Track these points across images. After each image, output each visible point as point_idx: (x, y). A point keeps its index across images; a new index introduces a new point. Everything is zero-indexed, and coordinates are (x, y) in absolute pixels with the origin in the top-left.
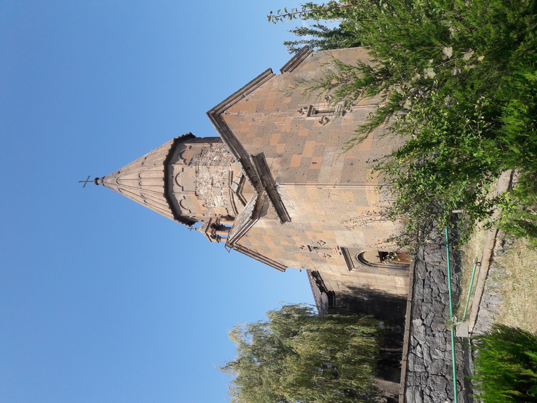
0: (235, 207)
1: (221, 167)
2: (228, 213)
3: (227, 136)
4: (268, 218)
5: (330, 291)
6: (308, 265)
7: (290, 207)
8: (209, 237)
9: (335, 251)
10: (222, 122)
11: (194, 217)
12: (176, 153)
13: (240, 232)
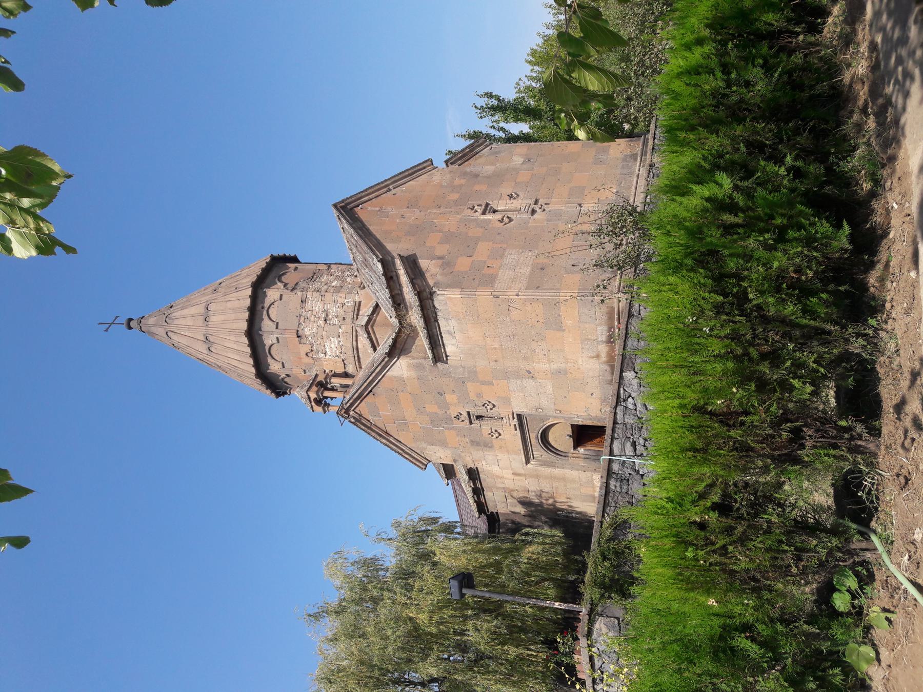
0: (358, 356)
1: (343, 296)
3: (363, 233)
4: (414, 358)
5: (492, 512)
6: (463, 454)
7: (449, 332)
8: (311, 402)
9: (508, 424)
10: (356, 217)
11: (288, 376)
12: (272, 275)
13: (366, 384)
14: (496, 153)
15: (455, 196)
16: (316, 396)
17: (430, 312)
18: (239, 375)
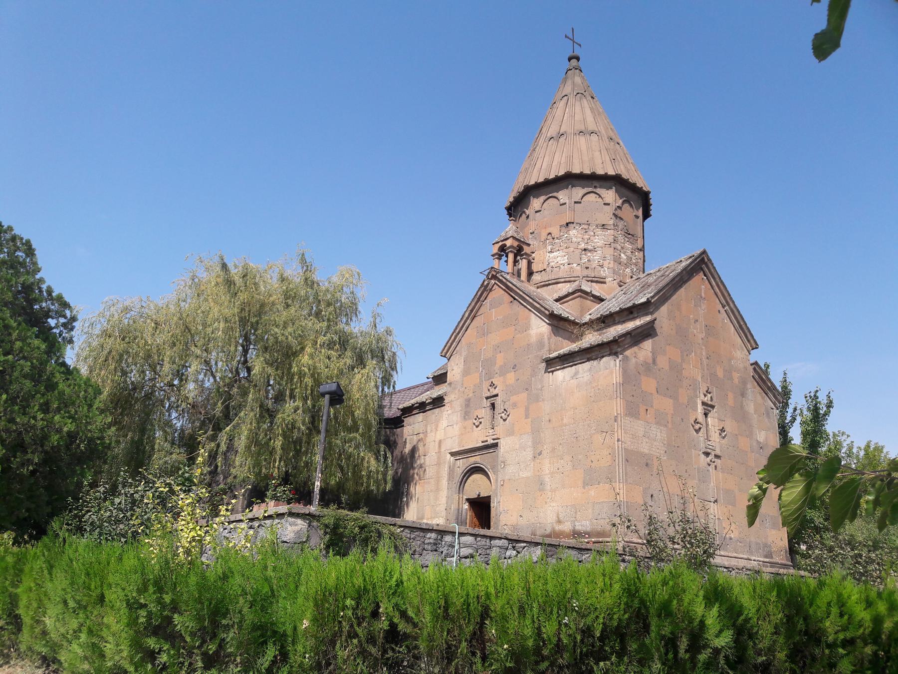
0: (549, 285)
1: (611, 266)
2: (537, 272)
3: (677, 281)
4: (549, 339)
5: (403, 421)
6: (457, 391)
7: (576, 373)
8: (502, 241)
9: (488, 434)
10: (693, 274)
11: (528, 217)
13: (521, 293)
14: (768, 414)
15: (720, 373)
16: (508, 245)
17: (596, 353)
18: (527, 170)
